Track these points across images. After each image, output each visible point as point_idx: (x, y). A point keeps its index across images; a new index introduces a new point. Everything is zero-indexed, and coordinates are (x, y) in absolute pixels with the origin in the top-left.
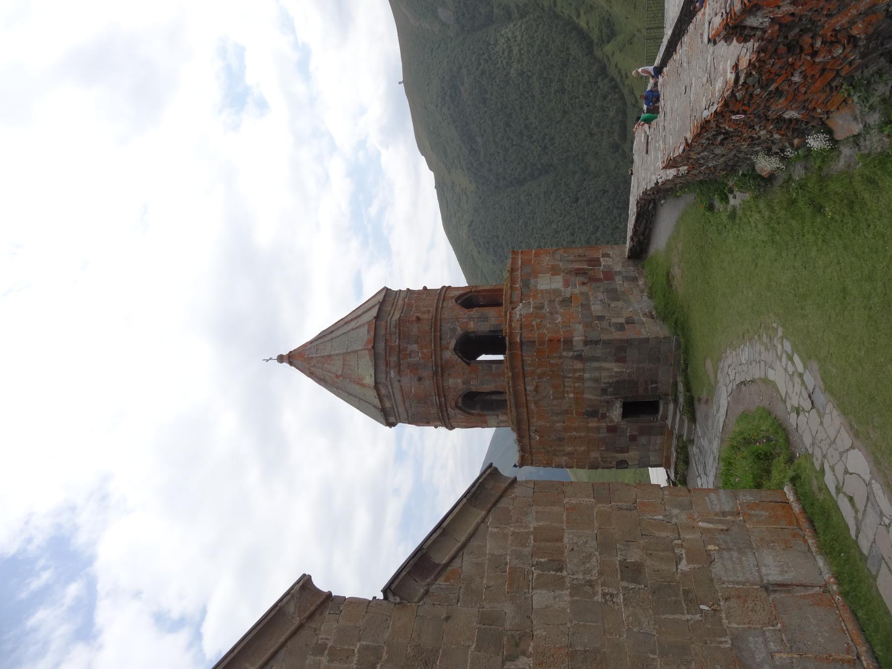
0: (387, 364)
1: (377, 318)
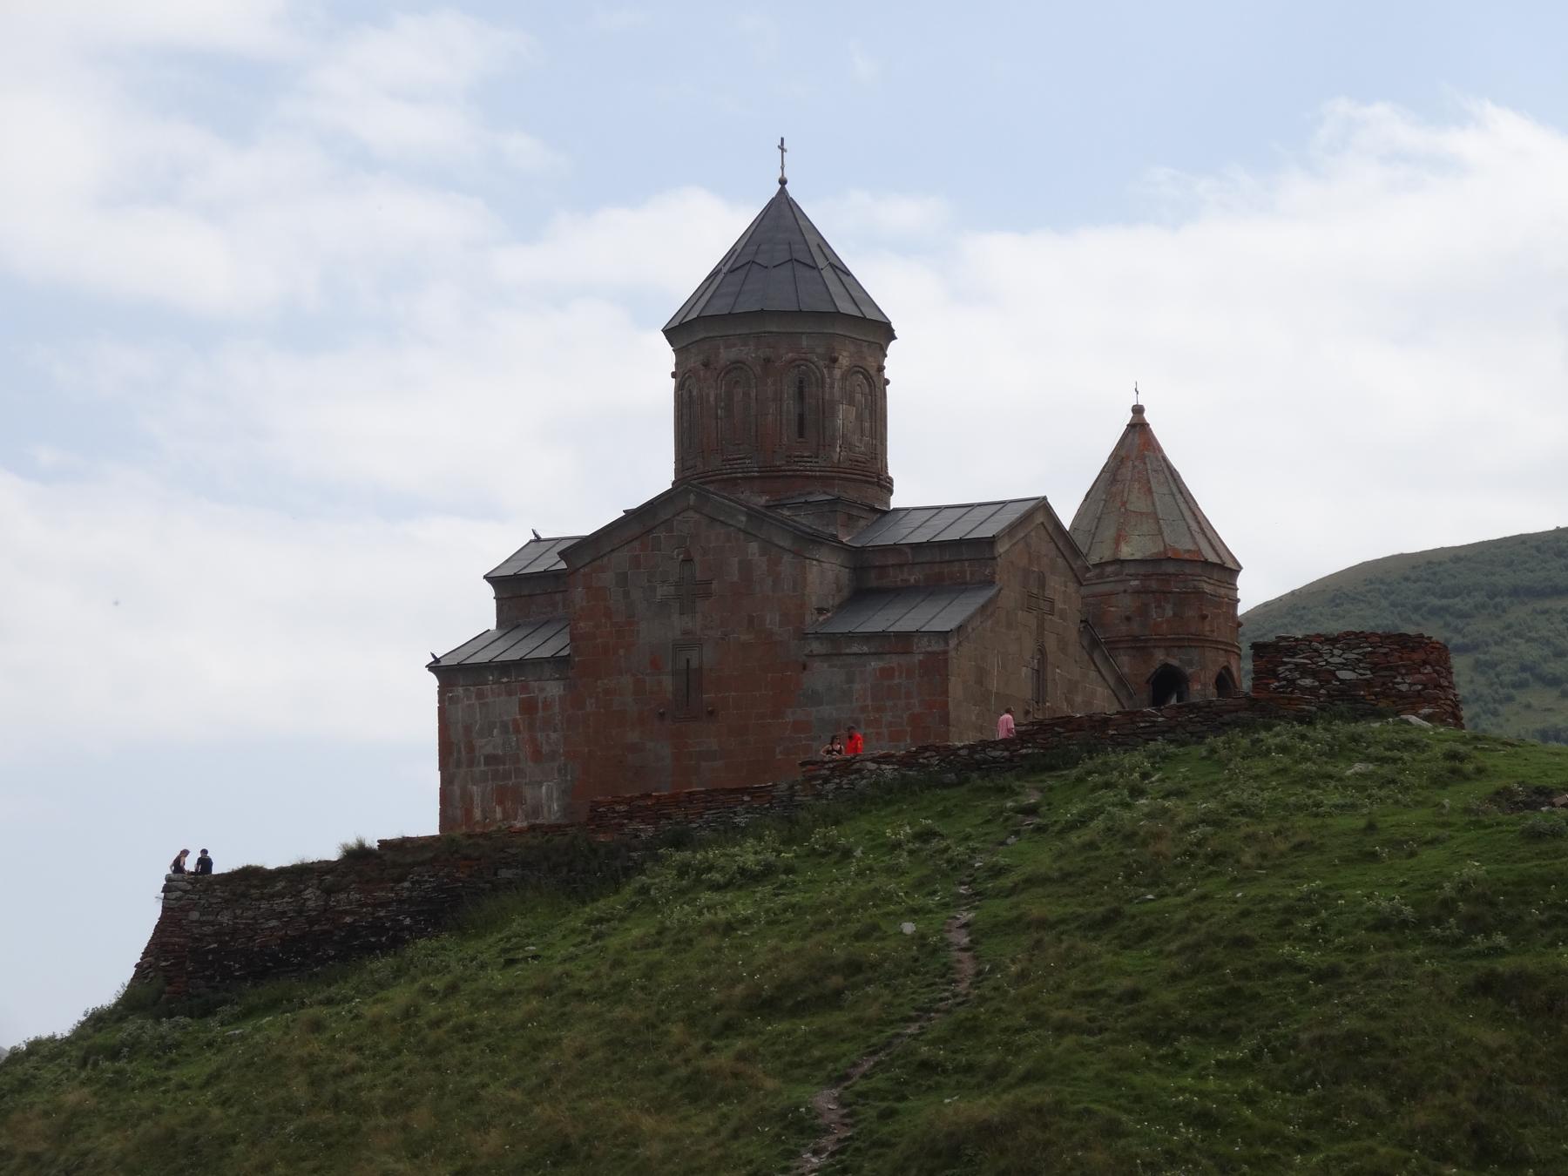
0: (1147, 576)
1: (1206, 562)
